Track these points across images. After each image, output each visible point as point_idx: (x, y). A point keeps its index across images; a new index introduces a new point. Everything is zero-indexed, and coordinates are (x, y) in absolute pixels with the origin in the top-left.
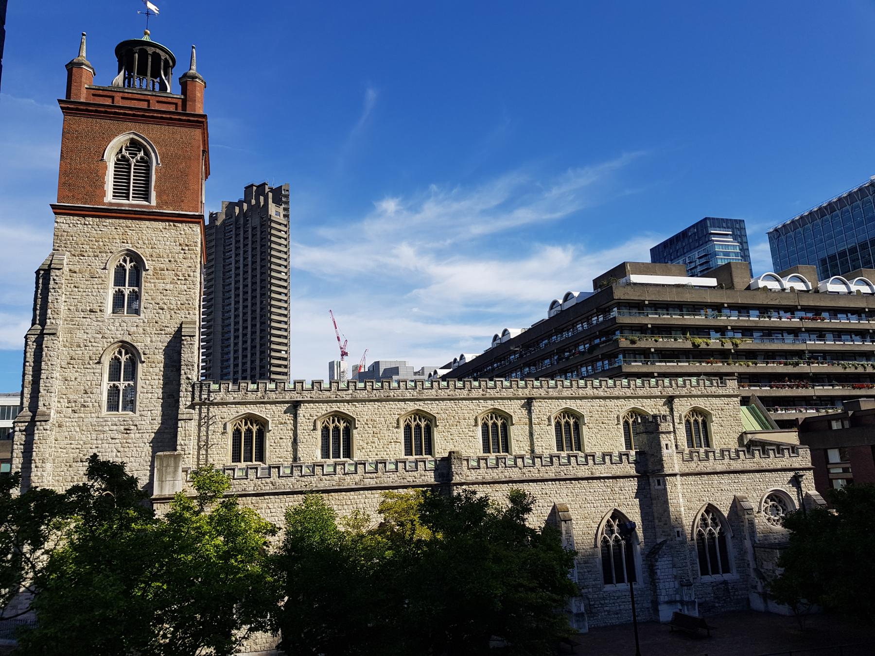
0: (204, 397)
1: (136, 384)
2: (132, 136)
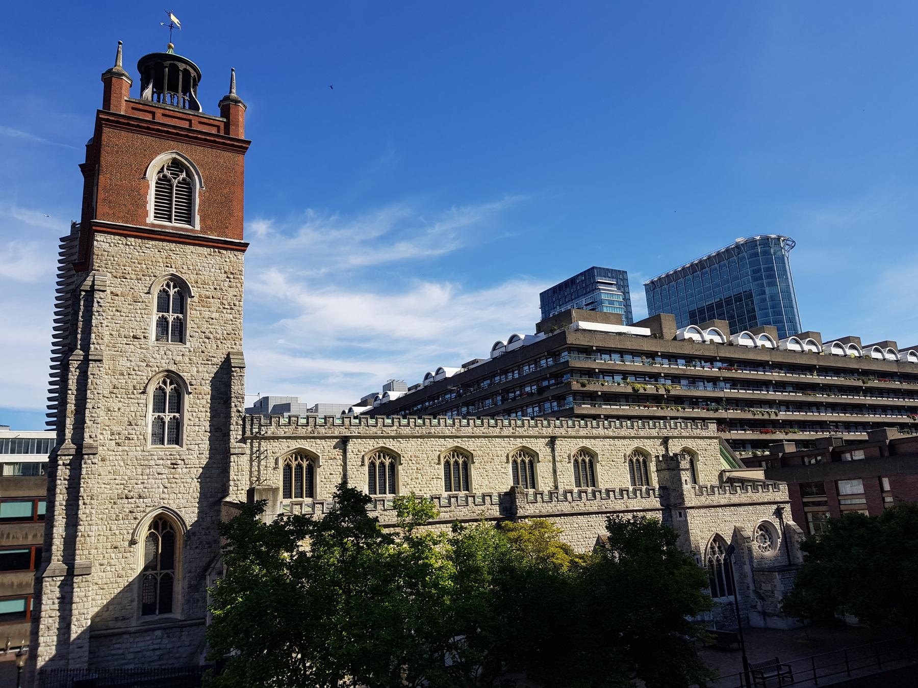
0: (255, 430)
1: (182, 416)
2: (174, 156)
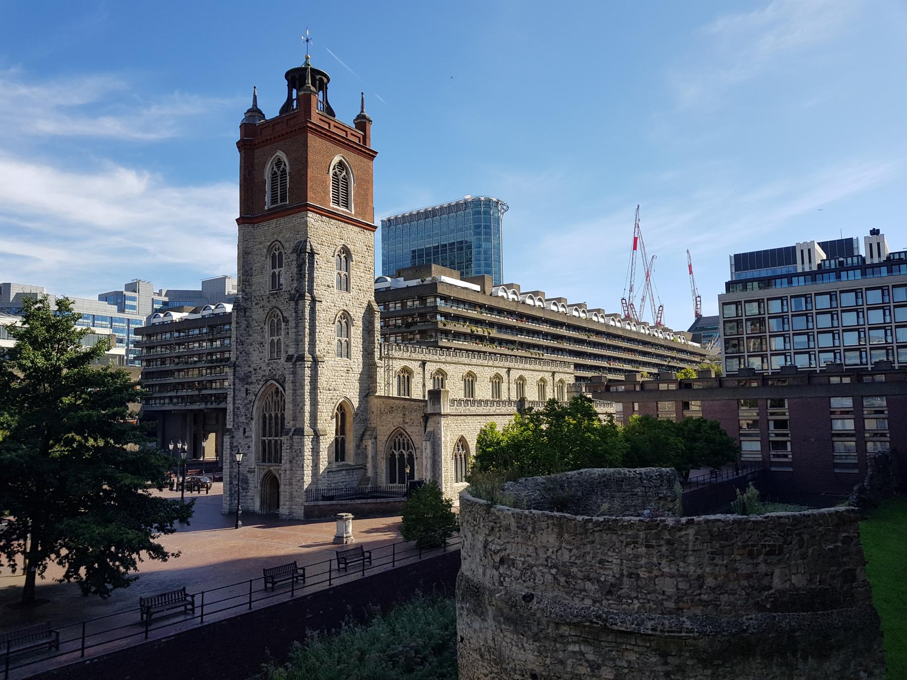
1: (350, 340)
